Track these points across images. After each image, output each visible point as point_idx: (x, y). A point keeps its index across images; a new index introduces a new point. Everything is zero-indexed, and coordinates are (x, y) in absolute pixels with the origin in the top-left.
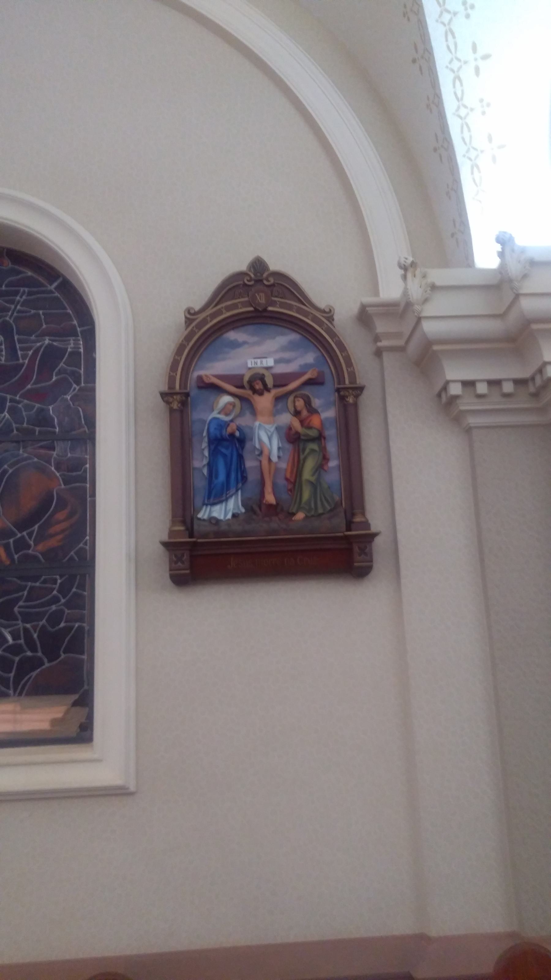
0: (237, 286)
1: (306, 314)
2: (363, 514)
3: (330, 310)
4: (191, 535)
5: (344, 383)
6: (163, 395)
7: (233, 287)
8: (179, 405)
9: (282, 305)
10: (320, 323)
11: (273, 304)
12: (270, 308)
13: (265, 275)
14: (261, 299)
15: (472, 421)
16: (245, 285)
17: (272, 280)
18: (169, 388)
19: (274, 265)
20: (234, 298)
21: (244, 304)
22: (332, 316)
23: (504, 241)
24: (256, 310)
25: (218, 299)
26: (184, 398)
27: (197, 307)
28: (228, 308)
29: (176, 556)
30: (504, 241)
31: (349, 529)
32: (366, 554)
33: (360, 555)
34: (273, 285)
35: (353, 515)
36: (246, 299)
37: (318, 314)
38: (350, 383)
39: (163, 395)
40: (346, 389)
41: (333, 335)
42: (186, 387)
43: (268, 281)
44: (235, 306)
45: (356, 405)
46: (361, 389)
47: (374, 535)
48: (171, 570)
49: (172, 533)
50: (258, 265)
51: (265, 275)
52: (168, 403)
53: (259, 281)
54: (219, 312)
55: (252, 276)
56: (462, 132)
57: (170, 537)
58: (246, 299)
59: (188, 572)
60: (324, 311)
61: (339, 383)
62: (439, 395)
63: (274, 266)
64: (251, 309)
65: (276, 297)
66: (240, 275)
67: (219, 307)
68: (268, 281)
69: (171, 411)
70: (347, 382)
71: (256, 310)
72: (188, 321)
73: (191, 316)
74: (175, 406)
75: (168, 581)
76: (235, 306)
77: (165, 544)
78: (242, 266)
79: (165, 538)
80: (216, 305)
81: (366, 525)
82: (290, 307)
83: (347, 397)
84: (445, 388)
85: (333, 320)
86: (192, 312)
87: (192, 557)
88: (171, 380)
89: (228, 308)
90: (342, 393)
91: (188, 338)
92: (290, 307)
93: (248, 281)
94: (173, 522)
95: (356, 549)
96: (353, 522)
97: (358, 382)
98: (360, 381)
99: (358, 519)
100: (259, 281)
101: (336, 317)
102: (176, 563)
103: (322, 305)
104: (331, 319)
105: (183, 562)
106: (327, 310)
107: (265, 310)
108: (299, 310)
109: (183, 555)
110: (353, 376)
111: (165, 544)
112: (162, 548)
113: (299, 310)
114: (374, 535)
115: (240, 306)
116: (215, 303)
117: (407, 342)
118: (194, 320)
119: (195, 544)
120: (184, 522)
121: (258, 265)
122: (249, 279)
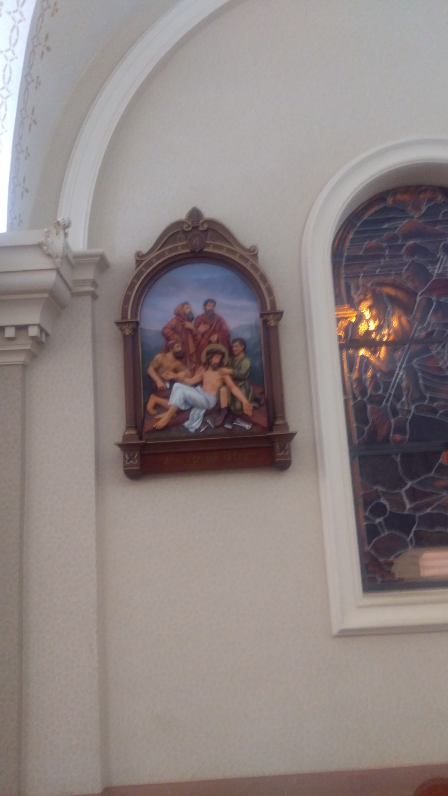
0: (178, 233)
1: (235, 253)
2: (283, 418)
3: (254, 250)
4: (141, 438)
6: (118, 324)
7: (173, 233)
8: (131, 332)
9: (215, 246)
10: (247, 260)
11: (208, 245)
12: (205, 250)
16: (184, 231)
17: (206, 226)
19: (209, 213)
21: (184, 247)
22: (256, 254)
24: (193, 252)
27: (145, 250)
29: (129, 455)
33: (281, 451)
34: (206, 231)
35: (275, 418)
36: (185, 243)
39: (118, 324)
41: (257, 269)
42: (136, 316)
45: (276, 328)
46: (281, 314)
47: (293, 435)
48: (125, 466)
49: (125, 437)
50: (195, 214)
52: (122, 330)
55: (190, 223)
56: (17, 41)
59: (138, 468)
60: (249, 250)
66: (179, 223)
69: (125, 336)
72: (138, 262)
76: (176, 249)
78: (181, 214)
81: (286, 426)
82: (221, 248)
86: (140, 254)
87: (142, 457)
89: (170, 251)
91: (137, 276)
92: (221, 248)
95: (277, 447)
97: (278, 309)
98: (280, 306)
99: (278, 422)
100: (195, 228)
102: (129, 461)
103: (248, 244)
104: (255, 256)
105: (134, 460)
106: (252, 249)
107: (201, 251)
108: (229, 250)
109: (134, 455)
110: (273, 303)
112: (118, 449)
113: (229, 250)
115: (180, 247)
118: (142, 261)
119: (145, 445)
120: (136, 427)
121: (195, 214)
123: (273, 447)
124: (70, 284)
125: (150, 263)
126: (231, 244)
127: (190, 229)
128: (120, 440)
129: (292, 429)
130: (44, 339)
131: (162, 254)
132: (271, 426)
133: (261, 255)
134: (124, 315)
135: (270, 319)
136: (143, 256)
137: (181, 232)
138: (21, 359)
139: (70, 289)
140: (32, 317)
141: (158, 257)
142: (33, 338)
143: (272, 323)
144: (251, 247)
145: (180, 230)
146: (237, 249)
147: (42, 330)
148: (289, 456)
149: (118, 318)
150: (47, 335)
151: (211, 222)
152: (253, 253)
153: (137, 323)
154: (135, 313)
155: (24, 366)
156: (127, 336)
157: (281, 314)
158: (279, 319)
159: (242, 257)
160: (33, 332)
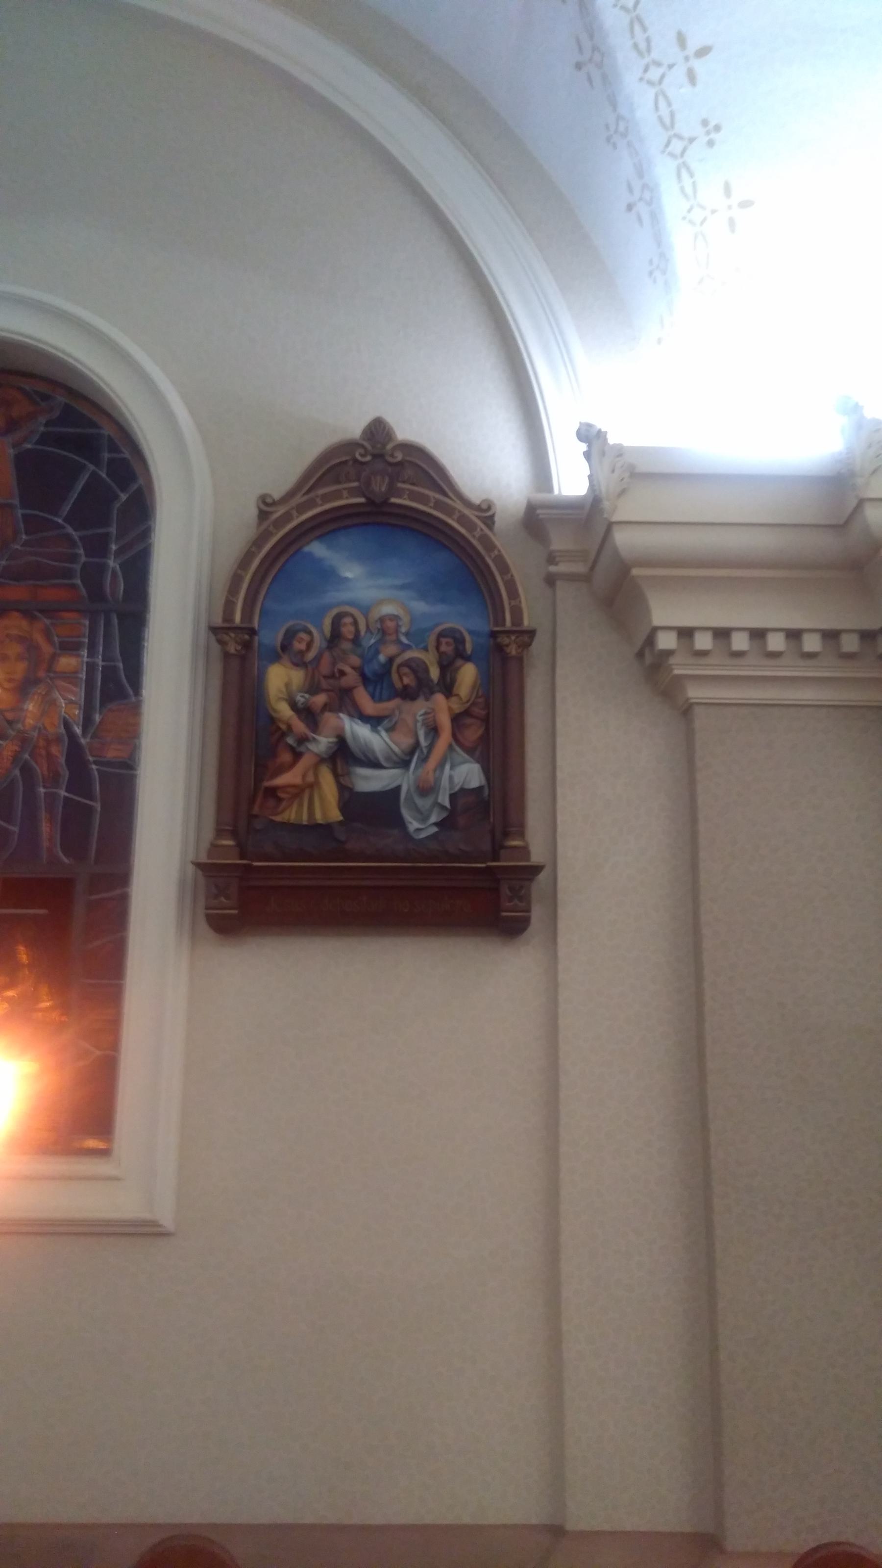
2: (521, 834)
3: (489, 508)
5: (504, 624)
6: (214, 630)
9: (413, 496)
10: (471, 527)
11: (399, 493)
12: (393, 500)
13: (389, 446)
14: (380, 486)
15: (695, 693)
16: (356, 461)
17: (399, 456)
18: (225, 620)
20: (338, 481)
21: (352, 492)
22: (493, 516)
23: (590, 436)
24: (371, 502)
25: (312, 482)
26: (247, 637)
28: (326, 498)
30: (590, 436)
31: (496, 858)
32: (521, 899)
33: (510, 899)
34: (400, 464)
35: (506, 834)
36: (355, 484)
37: (467, 512)
38: (513, 624)
39: (214, 630)
40: (508, 633)
43: (392, 456)
44: (337, 495)
45: (520, 660)
46: (532, 633)
47: (537, 869)
50: (378, 430)
51: (389, 446)
52: (220, 642)
53: (379, 456)
57: (210, 854)
58: (355, 484)
60: (478, 508)
61: (496, 624)
62: (640, 655)
63: (404, 432)
64: (362, 500)
65: (404, 482)
66: (348, 446)
67: (312, 495)
69: (226, 656)
72: (263, 515)
73: (266, 507)
75: (203, 926)
79: (204, 859)
81: (525, 851)
82: (424, 499)
83: (507, 645)
84: (650, 640)
85: (493, 523)
86: (269, 500)
88: (229, 606)
90: (499, 640)
91: (258, 542)
92: (424, 499)
93: (362, 455)
94: (220, 832)
95: (505, 890)
96: (502, 847)
101: (496, 519)
103: (476, 498)
104: (489, 521)
106: (484, 506)
107: (385, 502)
110: (517, 613)
113: (438, 505)
114: (537, 869)
117: (592, 568)
119: (248, 868)
120: (234, 834)
121: (378, 430)
122: (362, 451)
125: (287, 517)
126: (445, 494)
127: (368, 458)
134: (228, 614)
136: (274, 503)
137: (351, 463)
141: (301, 508)
143: (513, 650)
144: (485, 501)
145: (347, 458)
146: (458, 505)
148: (528, 911)
151: (410, 448)
156: (233, 655)
158: (527, 645)
159: (463, 520)
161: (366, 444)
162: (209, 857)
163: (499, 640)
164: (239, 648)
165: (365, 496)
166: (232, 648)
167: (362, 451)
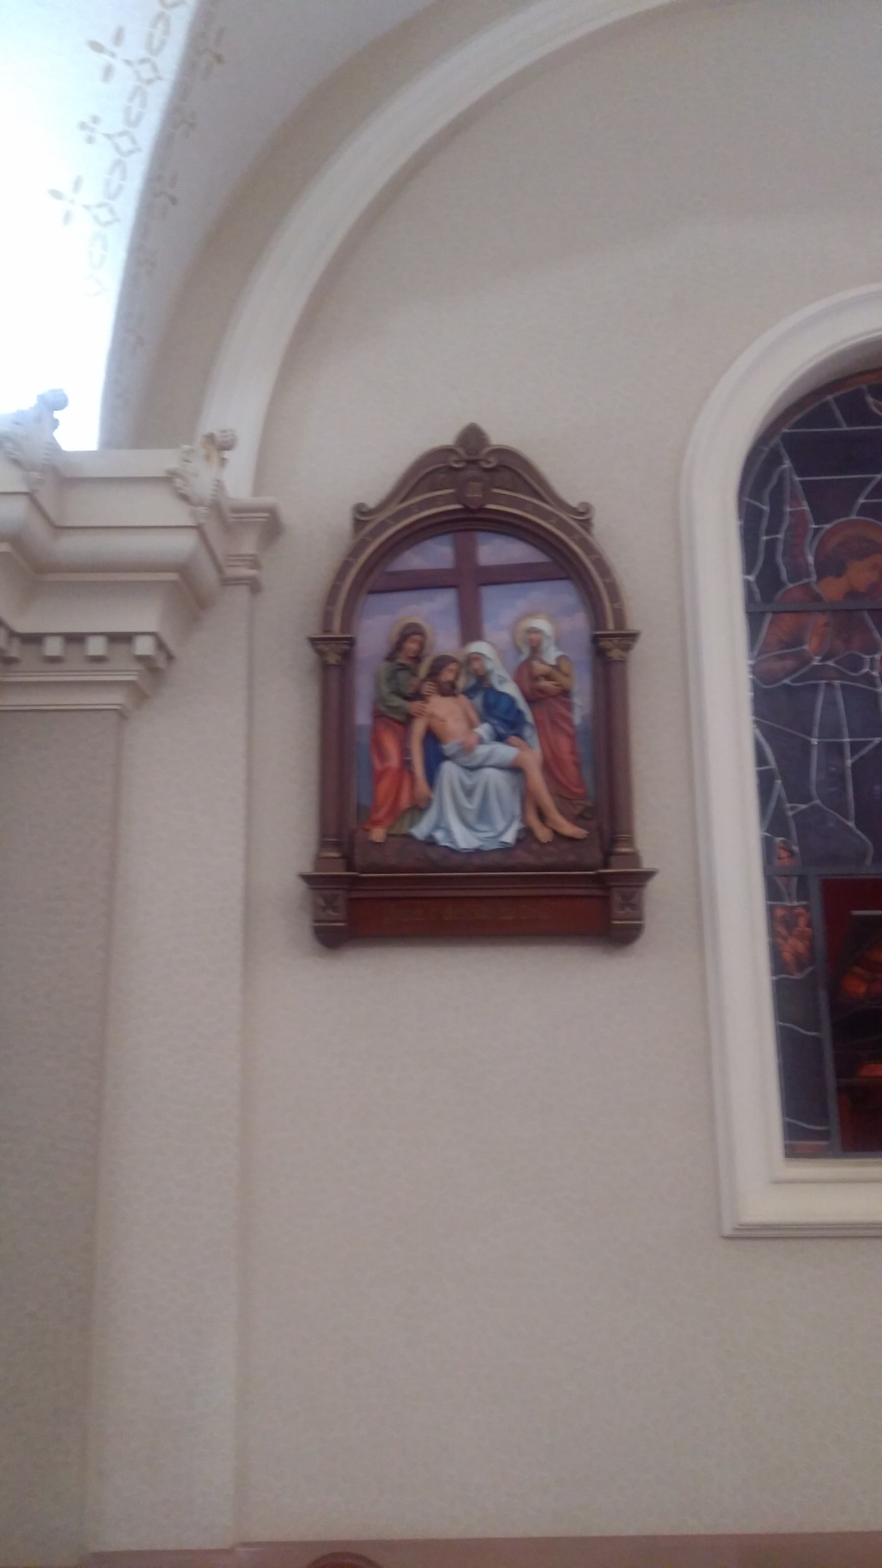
0: (437, 470)
1: (547, 516)
2: (630, 841)
4: (350, 867)
5: (605, 627)
6: (313, 641)
9: (512, 502)
11: (496, 499)
17: (493, 462)
19: (499, 435)
21: (447, 500)
24: (467, 509)
26: (347, 647)
27: (372, 502)
28: (422, 505)
31: (606, 865)
35: (614, 841)
37: (564, 516)
38: (616, 628)
39: (313, 641)
41: (590, 549)
43: (489, 462)
46: (633, 636)
47: (648, 875)
49: (319, 860)
50: (473, 436)
52: (321, 653)
54: (407, 512)
57: (317, 869)
68: (489, 462)
69: (325, 667)
70: (611, 625)
71: (467, 509)
73: (362, 516)
74: (333, 659)
77: (307, 878)
78: (447, 437)
79: (308, 869)
80: (403, 500)
81: (634, 858)
82: (521, 504)
83: (610, 650)
86: (364, 510)
88: (327, 617)
89: (422, 505)
90: (602, 644)
91: (355, 552)
92: (521, 504)
95: (617, 898)
103: (573, 499)
104: (587, 524)
105: (335, 909)
106: (582, 510)
107: (482, 510)
108: (537, 511)
110: (620, 616)
111: (307, 878)
112: (302, 886)
113: (537, 511)
114: (648, 875)
116: (402, 496)
120: (337, 845)
121: (473, 436)
122: (455, 458)
123: (606, 900)
124: (221, 558)
125: (383, 526)
128: (308, 868)
129: (647, 864)
130: (161, 662)
131: (407, 512)
132: (608, 856)
133: (599, 521)
135: (609, 647)
138: (116, 699)
139: (219, 570)
140: (143, 617)
142: (141, 659)
143: (615, 654)
147: (161, 645)
148: (640, 919)
149: (315, 631)
150: (170, 657)
152: (583, 516)
153: (351, 642)
154: (348, 621)
155: (122, 715)
157: (633, 636)
158: (627, 648)
159: (562, 524)
160: (144, 647)
161: (461, 451)
162: (316, 869)
163: (602, 644)
164: (339, 658)
165: (459, 503)
166: (333, 659)
167: (455, 458)
